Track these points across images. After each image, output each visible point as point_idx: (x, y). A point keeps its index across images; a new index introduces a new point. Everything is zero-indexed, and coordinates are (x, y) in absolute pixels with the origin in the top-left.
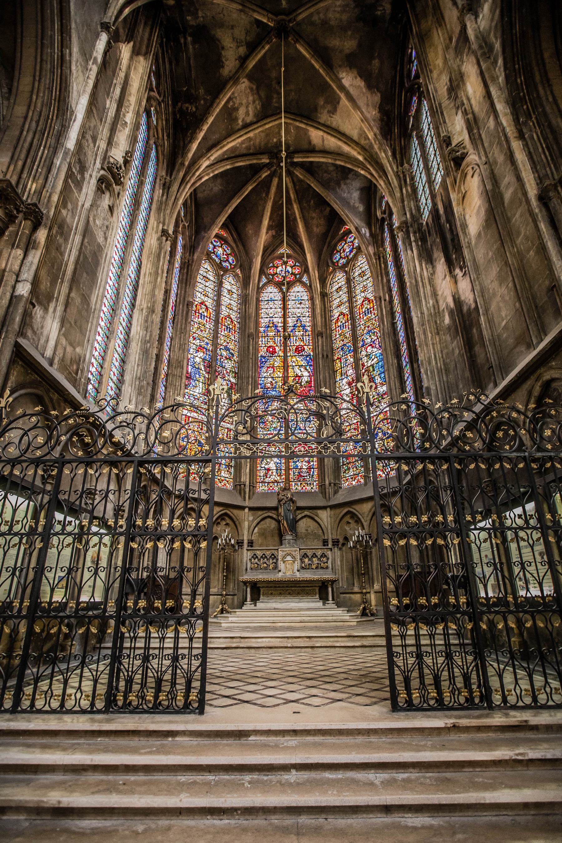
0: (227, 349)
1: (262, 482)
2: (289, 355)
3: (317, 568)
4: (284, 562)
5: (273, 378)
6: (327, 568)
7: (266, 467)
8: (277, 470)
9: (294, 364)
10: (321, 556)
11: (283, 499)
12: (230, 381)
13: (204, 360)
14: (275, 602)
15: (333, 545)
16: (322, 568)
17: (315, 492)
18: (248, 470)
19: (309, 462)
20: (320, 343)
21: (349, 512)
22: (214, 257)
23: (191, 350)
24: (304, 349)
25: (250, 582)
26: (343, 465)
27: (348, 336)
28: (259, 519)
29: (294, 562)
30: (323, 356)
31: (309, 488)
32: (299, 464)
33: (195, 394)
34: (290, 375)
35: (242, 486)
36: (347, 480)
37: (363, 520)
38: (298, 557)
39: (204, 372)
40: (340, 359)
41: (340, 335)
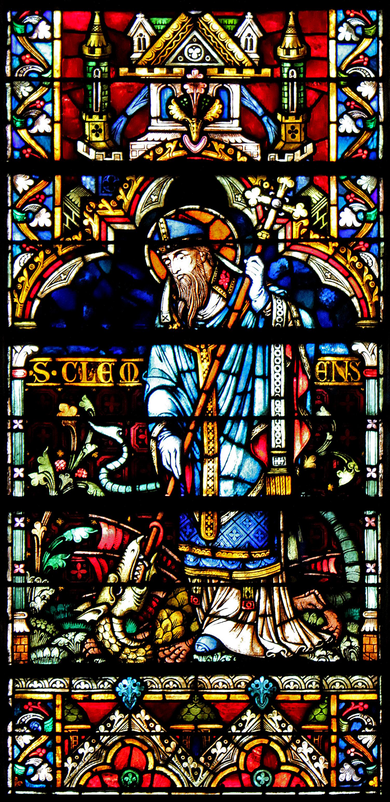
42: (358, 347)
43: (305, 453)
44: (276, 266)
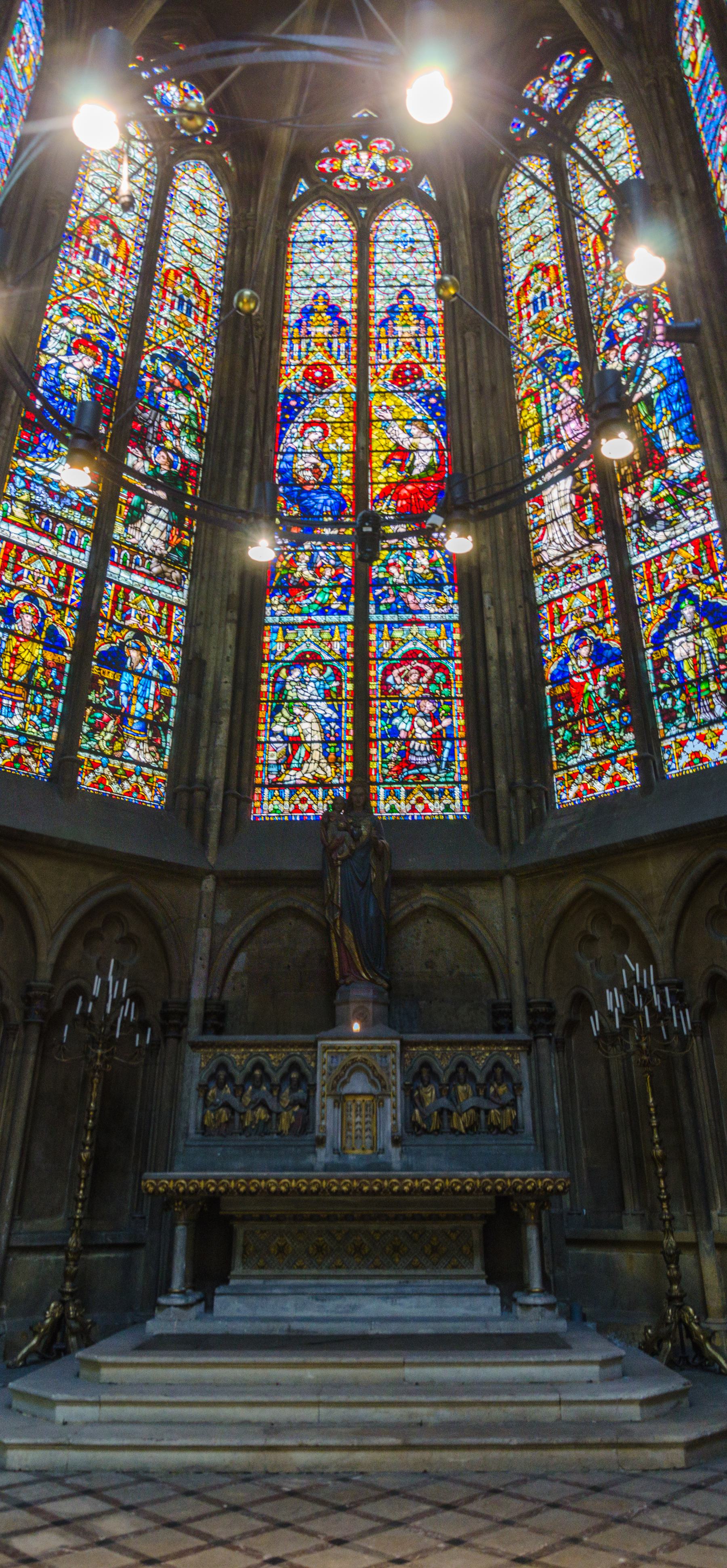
0: (174, 357)
1: (274, 785)
2: (372, 388)
3: (472, 1129)
4: (340, 1100)
5: (320, 454)
6: (515, 1128)
9: (388, 416)
10: (491, 1077)
11: (342, 841)
12: (179, 454)
14: (296, 1291)
15: (532, 1029)
16: (495, 1129)
18: (222, 738)
20: (471, 349)
21: (586, 897)
23: (52, 344)
24: (420, 373)
25: (188, 1198)
27: (559, 324)
28: (251, 920)
29: (379, 1099)
30: (481, 389)
31: (436, 807)
34: (375, 445)
35: (199, 795)
37: (644, 926)
38: (397, 1080)
40: (536, 395)
41: (534, 327)
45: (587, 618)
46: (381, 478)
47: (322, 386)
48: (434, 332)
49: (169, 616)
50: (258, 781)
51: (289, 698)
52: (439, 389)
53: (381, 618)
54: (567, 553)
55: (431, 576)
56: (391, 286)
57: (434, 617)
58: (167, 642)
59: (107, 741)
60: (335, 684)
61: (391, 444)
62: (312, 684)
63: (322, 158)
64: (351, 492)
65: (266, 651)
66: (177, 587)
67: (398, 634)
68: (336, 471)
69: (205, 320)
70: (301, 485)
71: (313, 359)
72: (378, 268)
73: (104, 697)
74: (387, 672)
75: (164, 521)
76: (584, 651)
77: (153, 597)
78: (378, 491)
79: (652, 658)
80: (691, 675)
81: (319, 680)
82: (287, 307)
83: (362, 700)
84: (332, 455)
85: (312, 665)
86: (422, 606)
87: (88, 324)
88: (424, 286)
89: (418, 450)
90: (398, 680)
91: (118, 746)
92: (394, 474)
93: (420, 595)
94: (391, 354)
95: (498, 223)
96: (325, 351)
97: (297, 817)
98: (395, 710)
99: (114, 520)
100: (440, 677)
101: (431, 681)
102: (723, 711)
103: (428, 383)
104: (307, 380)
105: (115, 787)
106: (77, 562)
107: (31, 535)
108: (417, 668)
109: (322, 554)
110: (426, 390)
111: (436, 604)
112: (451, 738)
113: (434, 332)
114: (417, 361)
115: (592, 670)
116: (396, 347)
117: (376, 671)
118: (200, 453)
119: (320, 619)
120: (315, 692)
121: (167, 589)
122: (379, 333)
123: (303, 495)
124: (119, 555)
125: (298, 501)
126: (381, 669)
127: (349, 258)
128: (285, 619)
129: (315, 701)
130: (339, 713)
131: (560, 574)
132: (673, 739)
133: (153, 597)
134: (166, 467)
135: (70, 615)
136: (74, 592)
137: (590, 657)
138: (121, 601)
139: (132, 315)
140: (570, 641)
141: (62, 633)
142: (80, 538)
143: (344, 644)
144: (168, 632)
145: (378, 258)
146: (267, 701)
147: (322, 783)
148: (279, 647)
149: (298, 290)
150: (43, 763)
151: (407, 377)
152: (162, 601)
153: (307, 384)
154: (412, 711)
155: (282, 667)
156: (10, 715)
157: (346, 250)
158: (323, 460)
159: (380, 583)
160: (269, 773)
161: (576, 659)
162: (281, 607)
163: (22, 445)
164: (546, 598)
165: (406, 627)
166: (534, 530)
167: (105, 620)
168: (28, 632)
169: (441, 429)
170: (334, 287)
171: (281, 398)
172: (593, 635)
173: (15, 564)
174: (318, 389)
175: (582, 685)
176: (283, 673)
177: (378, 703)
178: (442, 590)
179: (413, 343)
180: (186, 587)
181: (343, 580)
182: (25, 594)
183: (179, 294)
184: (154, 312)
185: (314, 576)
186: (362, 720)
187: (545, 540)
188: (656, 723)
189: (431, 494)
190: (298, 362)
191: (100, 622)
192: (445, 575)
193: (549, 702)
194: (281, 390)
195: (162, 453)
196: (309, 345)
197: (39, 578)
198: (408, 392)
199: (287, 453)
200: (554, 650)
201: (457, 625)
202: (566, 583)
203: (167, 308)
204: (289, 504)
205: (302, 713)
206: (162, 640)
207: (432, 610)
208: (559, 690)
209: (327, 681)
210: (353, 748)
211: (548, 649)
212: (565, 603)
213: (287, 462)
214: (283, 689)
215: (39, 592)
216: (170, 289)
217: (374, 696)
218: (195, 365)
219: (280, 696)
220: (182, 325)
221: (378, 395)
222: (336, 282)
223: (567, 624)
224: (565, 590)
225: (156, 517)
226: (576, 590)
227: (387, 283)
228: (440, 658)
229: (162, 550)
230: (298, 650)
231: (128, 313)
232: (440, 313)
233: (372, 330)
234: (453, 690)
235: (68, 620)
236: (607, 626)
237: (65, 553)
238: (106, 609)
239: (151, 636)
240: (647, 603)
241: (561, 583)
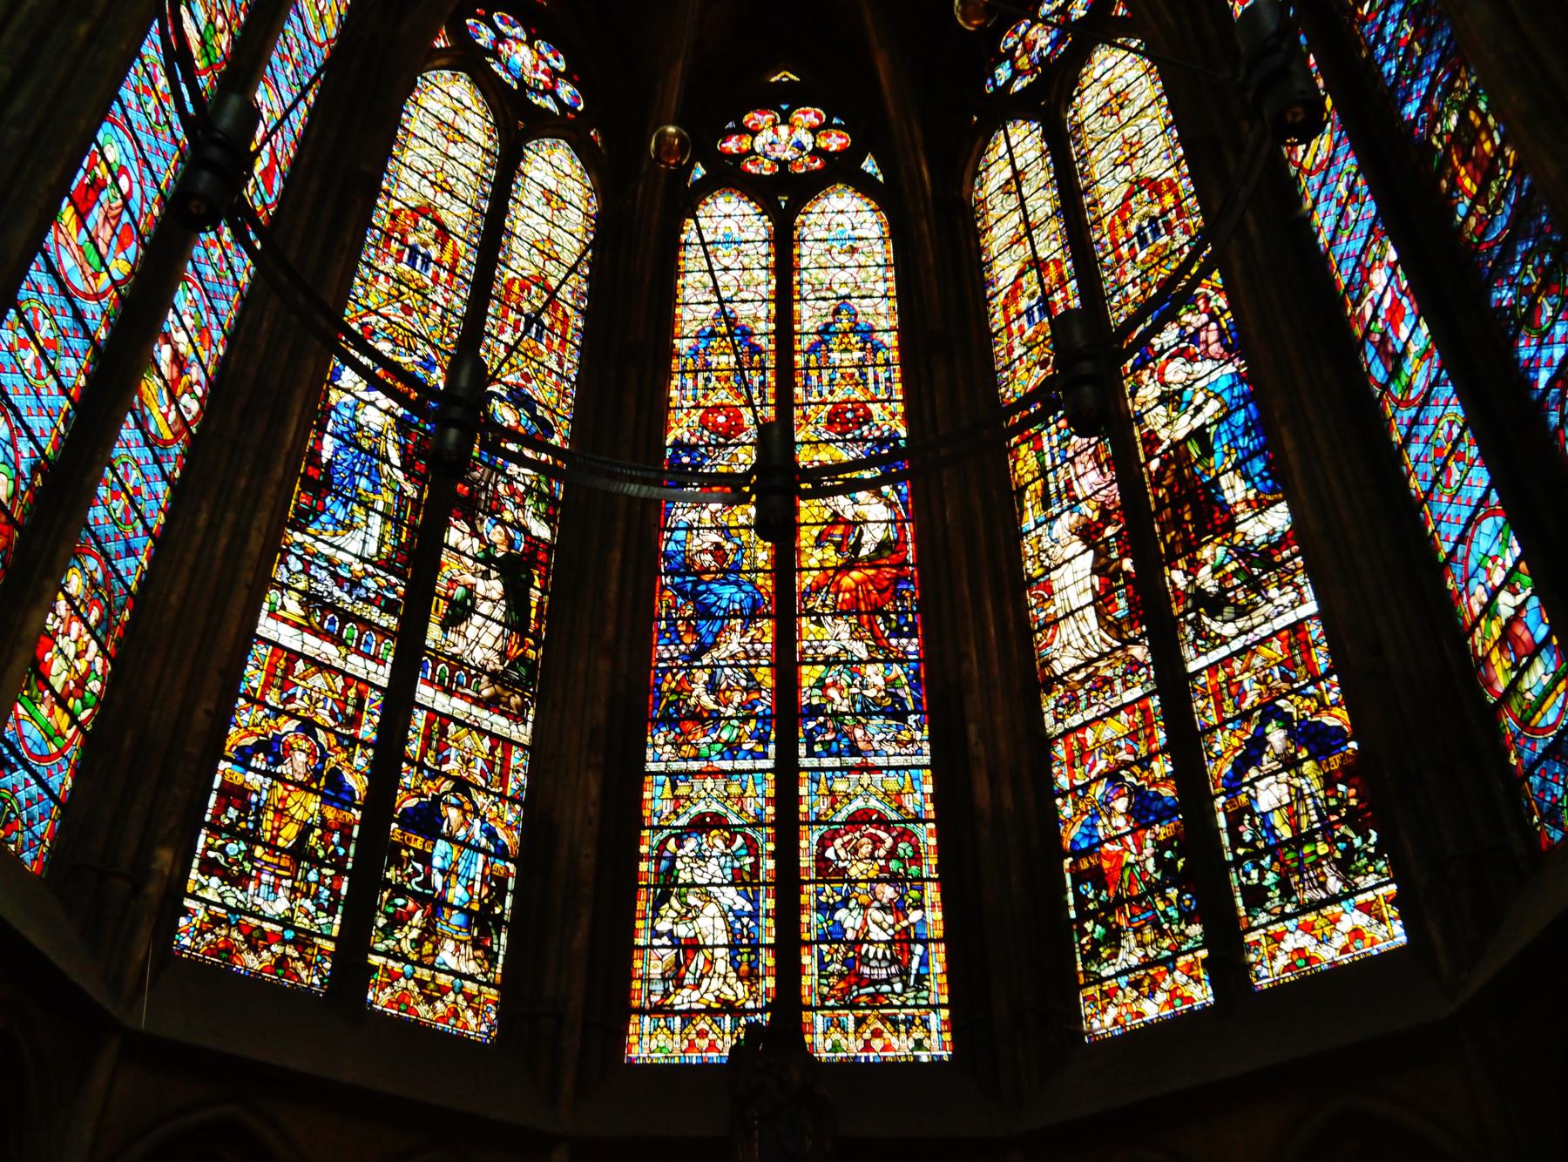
0: (518, 398)
5: (724, 530)
7: (682, 931)
8: (733, 947)
12: (525, 530)
13: (402, 425)
17: (936, 1063)
19: (896, 908)
22: (494, 67)
24: (868, 417)
26: (1084, 915)
32: (850, 920)
33: (341, 556)
36: (1109, 995)
39: (399, 475)
42: (508, 864)
43: (486, 897)
44: (484, 826)
45: (1123, 756)
46: (814, 563)
47: (728, 437)
48: (887, 360)
49: (506, 760)
50: (636, 1003)
51: (680, 881)
52: (894, 437)
53: (814, 762)
54: (1089, 662)
55: (888, 701)
56: (824, 299)
57: (894, 761)
58: (502, 797)
59: (412, 941)
60: (752, 860)
61: (827, 514)
62: (714, 861)
63: (727, 135)
64: (769, 582)
65: (646, 813)
66: (518, 718)
67: (840, 786)
68: (748, 553)
69: (562, 345)
70: (698, 574)
71: (713, 400)
72: (805, 275)
73: (408, 875)
74: (824, 843)
75: (499, 623)
76: (1121, 804)
77: (482, 732)
78: (809, 581)
79: (1224, 809)
80: (1285, 832)
81: (723, 854)
82: (677, 330)
83: (787, 883)
84: (742, 531)
85: (714, 832)
86: (876, 745)
87: (397, 349)
88: (871, 297)
89: (866, 522)
90: (842, 853)
91: (428, 948)
92: (830, 555)
93: (872, 729)
94: (826, 391)
95: (973, 211)
96: (731, 388)
97: (694, 1058)
98: (838, 898)
99: (427, 621)
100: (904, 848)
101: (892, 854)
102: (1339, 885)
103: (879, 428)
104: (705, 427)
105: (423, 1009)
106: (373, 678)
107: (308, 637)
108: (871, 836)
109: (728, 671)
110: (875, 439)
111: (898, 742)
112: (925, 942)
113: (887, 360)
114: (862, 399)
115: (1133, 832)
116: (831, 380)
117: (808, 841)
118: (552, 529)
119: (726, 765)
120: (719, 873)
121: (503, 721)
122: (808, 361)
123: (702, 588)
124: (434, 670)
125: (693, 596)
126: (816, 837)
127: (764, 263)
128: (675, 766)
129: (719, 886)
130: (754, 901)
131: (1081, 692)
132: (1262, 931)
133: (482, 732)
134: (504, 548)
135: (362, 755)
136: (370, 721)
137: (1129, 813)
138: (436, 737)
139: (460, 337)
140: (1098, 790)
141: (349, 779)
142: (378, 645)
143: (761, 801)
144: (504, 783)
145: (804, 263)
146: (648, 887)
147: (728, 1007)
148: (666, 807)
149: (693, 307)
150: (319, 971)
151: (849, 421)
152: (495, 738)
153: (706, 433)
154: (864, 899)
155: (670, 836)
156: (272, 896)
157: (760, 253)
158: (727, 539)
159: (815, 711)
160: (650, 992)
161: (1109, 816)
162: (668, 748)
163: (300, 512)
164: (1060, 728)
165: (854, 777)
166: (1040, 630)
167: (411, 763)
168: (300, 777)
169: (899, 493)
170: (744, 301)
171: (669, 452)
172: (1133, 780)
173: (284, 678)
174: (721, 440)
175: (1119, 856)
176: (671, 845)
177: (810, 888)
178: (905, 721)
179: (857, 374)
180: (530, 718)
181: (759, 709)
182: (298, 723)
183: (526, 312)
184: (490, 335)
185: (716, 702)
186: (788, 915)
187: (1056, 644)
188: (1235, 908)
189: (886, 583)
190: (692, 403)
191: (404, 765)
192: (910, 698)
193: (1069, 883)
194: (668, 443)
195: (499, 528)
196: (708, 380)
197: (318, 700)
198: (851, 441)
199: (677, 529)
200: (1075, 804)
201: (928, 772)
202: (1089, 705)
203: (509, 330)
204: (680, 600)
205: (700, 904)
206: (495, 794)
207: (891, 752)
208: (1084, 865)
209: (735, 857)
210: (776, 956)
211: (1065, 804)
212: (1089, 735)
213: (677, 542)
214: (672, 867)
215: (318, 720)
216: (513, 304)
217: (806, 878)
218: (547, 407)
219: (665, 880)
220: (530, 354)
221: (807, 446)
222: (745, 295)
223: (1093, 766)
224: (1089, 715)
225: (488, 617)
226: (1105, 715)
227: (818, 295)
228: (905, 821)
229: (495, 664)
230: (694, 811)
231: (455, 335)
232: (895, 333)
233: (797, 358)
234: (925, 870)
235: (359, 762)
236: (1154, 765)
237: (356, 665)
238: (413, 747)
239: (479, 789)
240: (1214, 728)
241: (1083, 705)
